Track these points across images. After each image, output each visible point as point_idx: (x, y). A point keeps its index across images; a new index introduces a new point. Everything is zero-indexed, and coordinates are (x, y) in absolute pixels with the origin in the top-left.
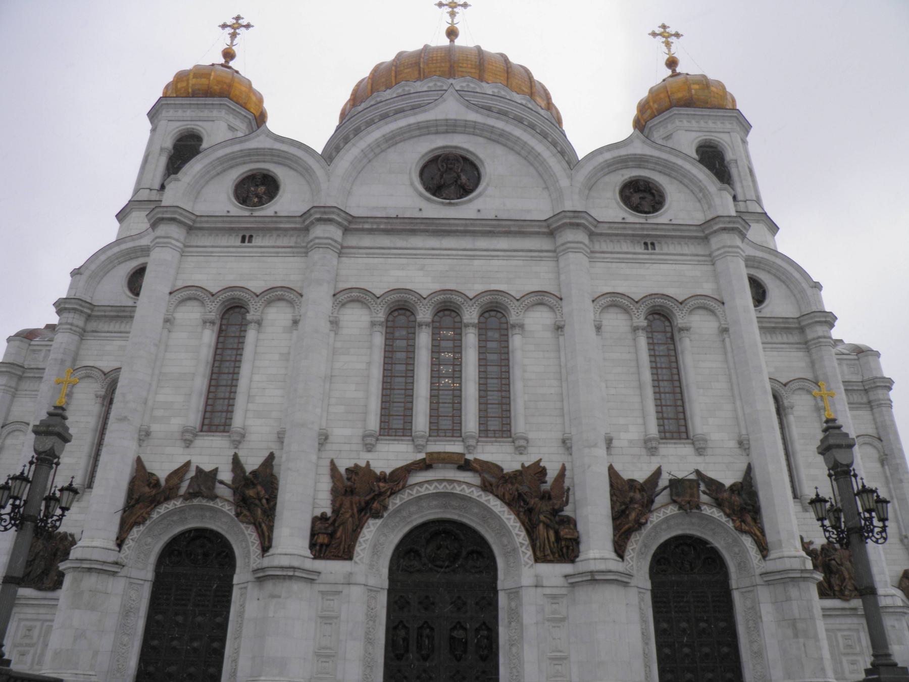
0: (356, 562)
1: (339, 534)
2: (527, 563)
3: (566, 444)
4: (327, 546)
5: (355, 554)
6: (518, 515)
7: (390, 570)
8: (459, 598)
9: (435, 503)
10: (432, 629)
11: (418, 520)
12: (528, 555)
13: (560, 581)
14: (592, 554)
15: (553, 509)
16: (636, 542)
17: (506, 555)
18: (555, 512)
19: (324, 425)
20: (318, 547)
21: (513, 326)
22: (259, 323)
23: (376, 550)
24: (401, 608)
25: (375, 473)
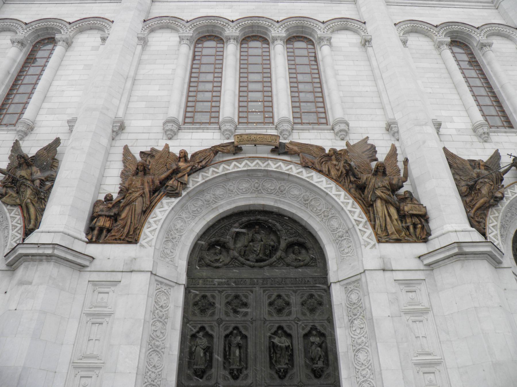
0: (142, 246)
1: (123, 215)
2: (369, 243)
3: (391, 128)
4: (109, 231)
5: (142, 236)
6: (349, 191)
7: (190, 264)
8: (279, 296)
9: (245, 185)
10: (245, 337)
11: (226, 206)
12: (367, 235)
13: (415, 264)
14: (448, 227)
15: (391, 184)
16: (496, 218)
17: (338, 240)
18: (394, 188)
19: (120, 114)
20: (96, 232)
21: (321, 39)
22: (69, 44)
23: (170, 237)
24: (203, 311)
25: (174, 155)
